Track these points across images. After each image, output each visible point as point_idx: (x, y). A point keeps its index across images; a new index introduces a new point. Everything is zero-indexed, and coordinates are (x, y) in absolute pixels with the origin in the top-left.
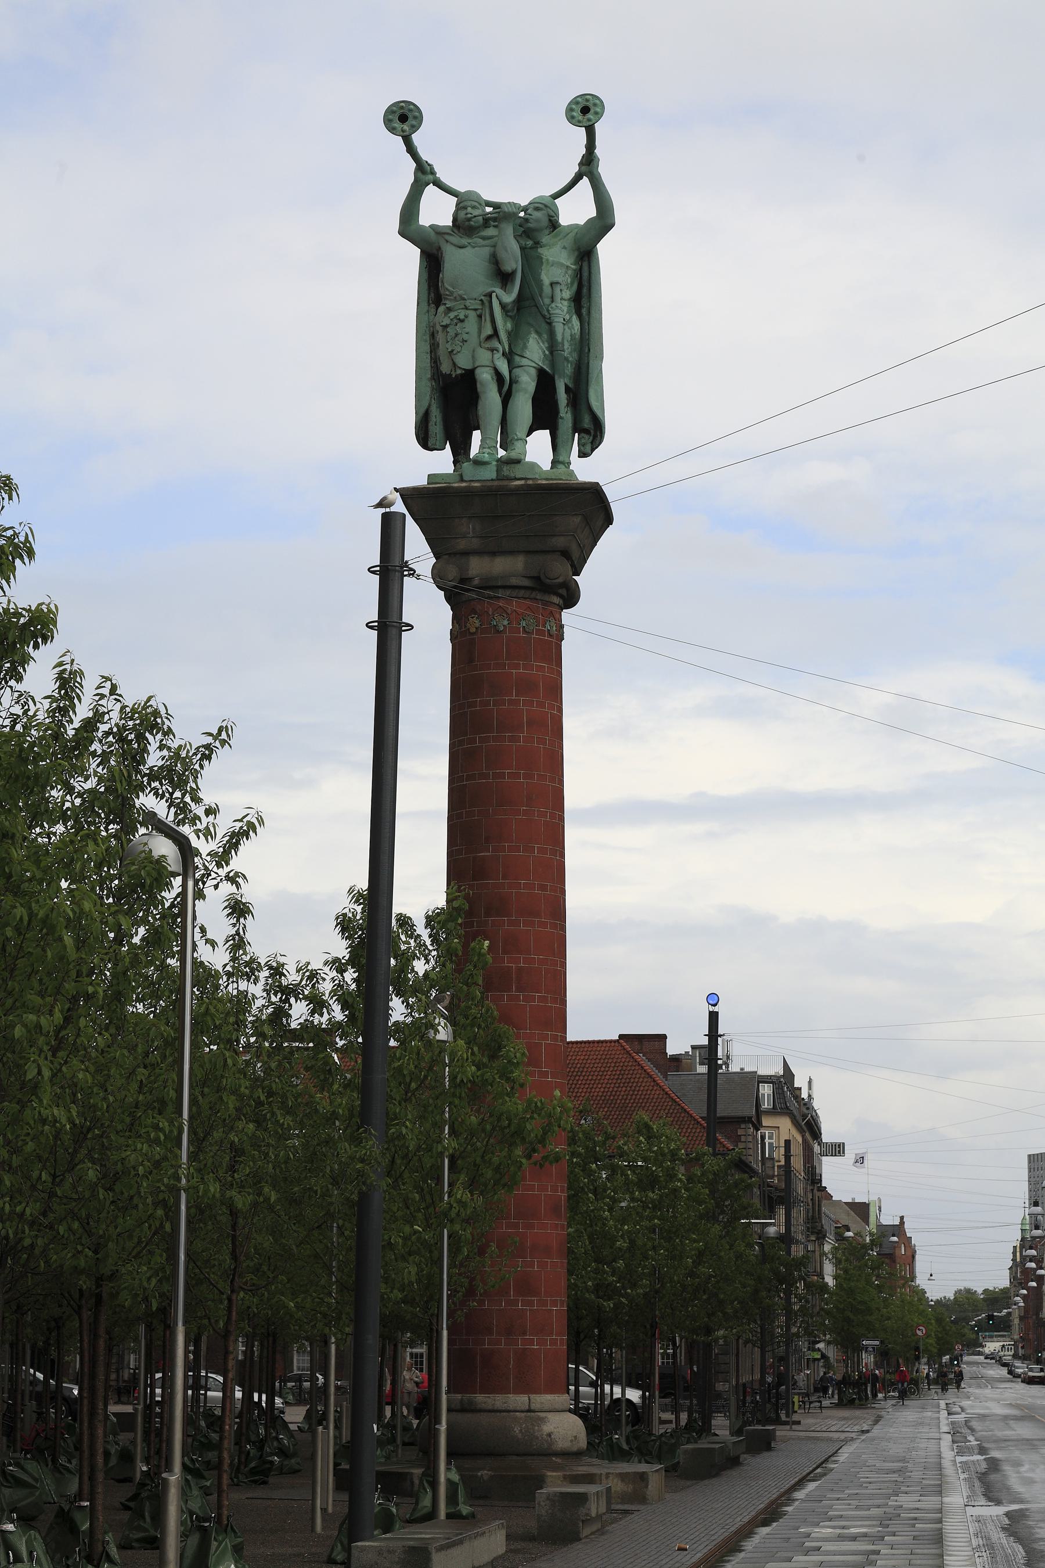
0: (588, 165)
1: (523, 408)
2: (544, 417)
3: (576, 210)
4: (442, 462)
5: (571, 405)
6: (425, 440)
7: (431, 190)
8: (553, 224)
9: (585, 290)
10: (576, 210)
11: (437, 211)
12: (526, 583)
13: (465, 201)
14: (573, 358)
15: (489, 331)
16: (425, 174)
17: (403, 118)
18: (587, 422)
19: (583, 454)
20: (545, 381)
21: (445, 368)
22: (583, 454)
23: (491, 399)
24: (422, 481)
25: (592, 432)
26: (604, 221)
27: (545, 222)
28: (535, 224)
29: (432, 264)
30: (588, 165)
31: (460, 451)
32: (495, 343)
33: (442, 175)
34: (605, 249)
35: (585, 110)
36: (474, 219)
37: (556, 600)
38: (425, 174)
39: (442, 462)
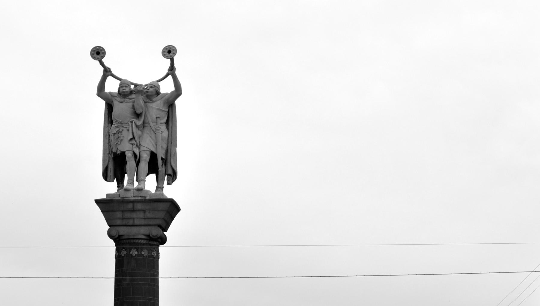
0: (172, 70)
1: (144, 166)
2: (153, 168)
3: (167, 87)
4: (112, 188)
5: (163, 165)
6: (106, 177)
7: (110, 78)
8: (158, 93)
9: (170, 119)
10: (167, 87)
11: (112, 86)
12: (143, 237)
13: (124, 84)
14: (165, 146)
15: (131, 137)
16: (107, 72)
17: (98, 53)
18: (170, 172)
19: (169, 184)
20: (153, 156)
21: (114, 150)
22: (169, 184)
23: (131, 163)
24: (104, 197)
25: (173, 176)
26: (178, 92)
27: (155, 93)
28: (151, 92)
29: (109, 108)
30: (172, 70)
31: (120, 183)
32: (133, 142)
33: (114, 72)
34: (178, 102)
35: (169, 52)
36: (127, 91)
37: (156, 243)
38: (107, 72)
39: (112, 188)
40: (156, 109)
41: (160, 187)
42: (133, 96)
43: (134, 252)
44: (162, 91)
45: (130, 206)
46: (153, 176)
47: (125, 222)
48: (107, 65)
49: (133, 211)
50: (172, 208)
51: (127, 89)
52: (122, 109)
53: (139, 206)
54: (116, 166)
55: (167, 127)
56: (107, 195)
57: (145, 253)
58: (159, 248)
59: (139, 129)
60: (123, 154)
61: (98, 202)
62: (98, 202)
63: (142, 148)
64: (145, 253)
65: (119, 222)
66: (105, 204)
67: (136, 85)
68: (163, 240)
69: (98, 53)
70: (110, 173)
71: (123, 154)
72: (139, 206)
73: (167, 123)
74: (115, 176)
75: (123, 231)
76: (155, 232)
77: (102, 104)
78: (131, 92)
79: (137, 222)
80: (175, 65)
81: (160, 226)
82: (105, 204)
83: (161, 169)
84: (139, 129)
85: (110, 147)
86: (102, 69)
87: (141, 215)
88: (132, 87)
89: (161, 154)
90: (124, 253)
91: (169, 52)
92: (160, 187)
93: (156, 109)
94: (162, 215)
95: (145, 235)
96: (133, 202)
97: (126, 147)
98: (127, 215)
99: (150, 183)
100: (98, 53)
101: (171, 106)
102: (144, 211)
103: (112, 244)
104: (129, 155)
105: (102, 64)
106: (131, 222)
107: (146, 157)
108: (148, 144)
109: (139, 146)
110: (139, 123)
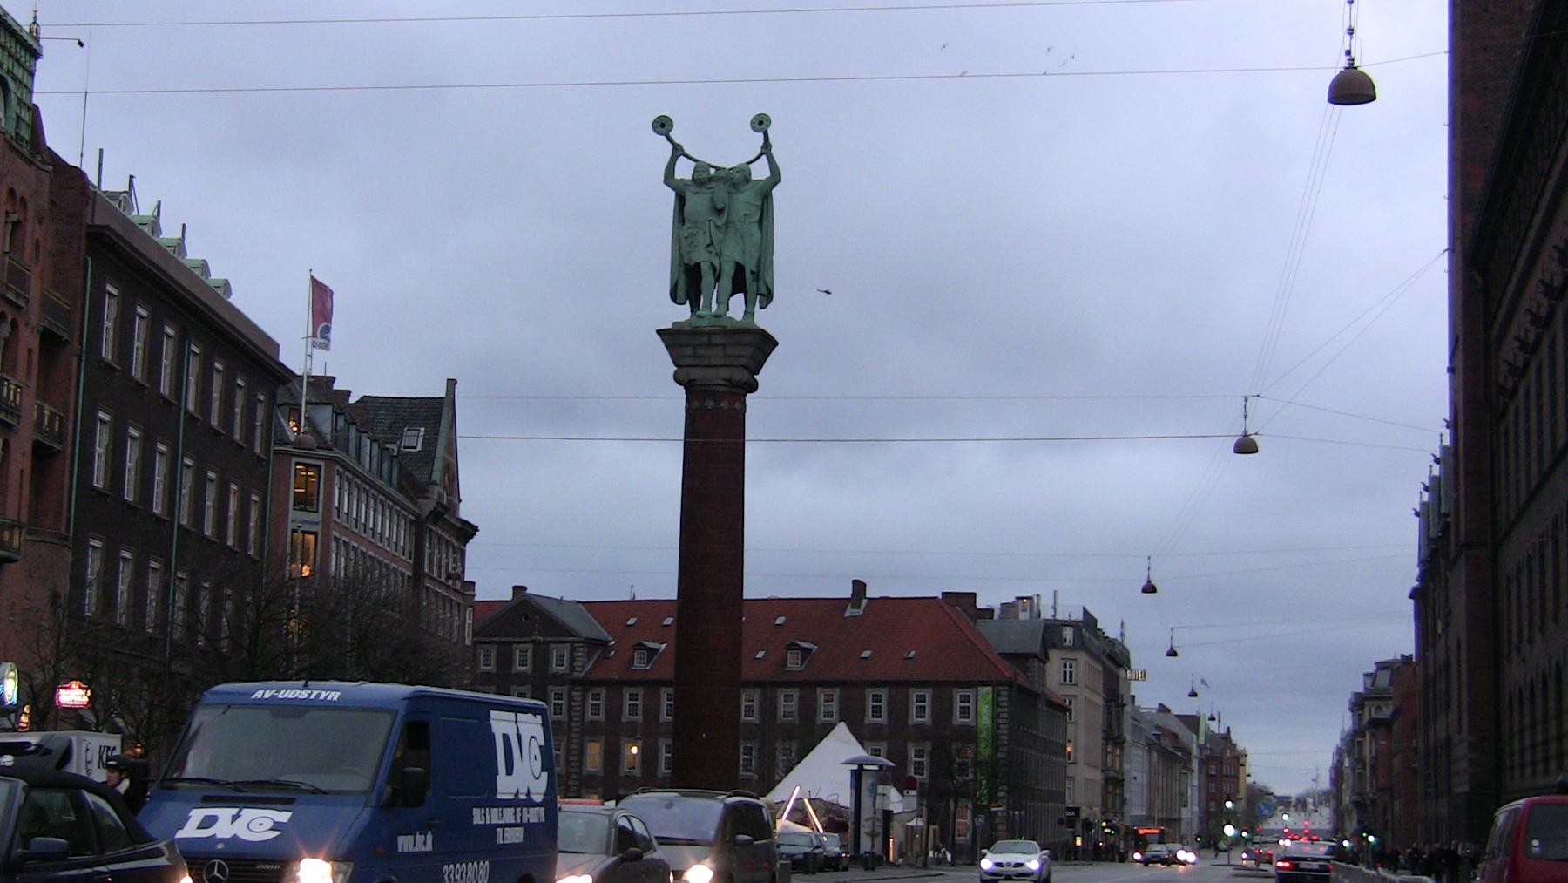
0: (767, 145)
1: (726, 282)
2: (738, 286)
3: (760, 171)
4: (683, 313)
5: (753, 281)
6: (674, 297)
7: (681, 160)
8: (747, 180)
10: (760, 171)
11: (684, 170)
13: (701, 167)
16: (678, 151)
17: (663, 126)
18: (764, 290)
20: (740, 268)
23: (707, 278)
25: (767, 297)
26: (775, 178)
28: (737, 179)
29: (681, 200)
30: (767, 145)
31: (695, 307)
33: (687, 150)
35: (761, 123)
36: (705, 178)
38: (678, 151)
39: (683, 313)
40: (744, 202)
41: (749, 312)
42: (713, 185)
43: (710, 404)
44: (754, 177)
45: (705, 339)
46: (740, 297)
47: (697, 362)
48: (677, 141)
49: (710, 345)
50: (766, 343)
51: (705, 175)
52: (698, 203)
53: (716, 339)
54: (688, 283)
55: (761, 228)
57: (724, 405)
59: (722, 231)
60: (698, 265)
61: (658, 332)
62: (658, 332)
63: (724, 258)
64: (724, 405)
65: (690, 361)
67: (717, 169)
68: (753, 387)
69: (663, 125)
70: (681, 293)
71: (698, 265)
72: (716, 339)
73: (760, 221)
74: (688, 297)
75: (696, 374)
76: (741, 375)
77: (671, 195)
78: (711, 179)
79: (714, 362)
80: (771, 140)
81: (746, 367)
83: (751, 286)
84: (722, 231)
85: (681, 256)
86: (671, 147)
87: (720, 351)
88: (712, 171)
89: (750, 266)
90: (696, 404)
91: (761, 123)
92: (749, 312)
93: (744, 202)
94: (748, 351)
96: (709, 333)
97: (700, 256)
98: (701, 352)
99: (737, 307)
100: (663, 125)
101: (766, 197)
102: (723, 345)
103: (682, 389)
104: (705, 267)
105: (670, 139)
106: (706, 362)
107: (728, 271)
108: (733, 252)
109: (719, 255)
110: (721, 222)
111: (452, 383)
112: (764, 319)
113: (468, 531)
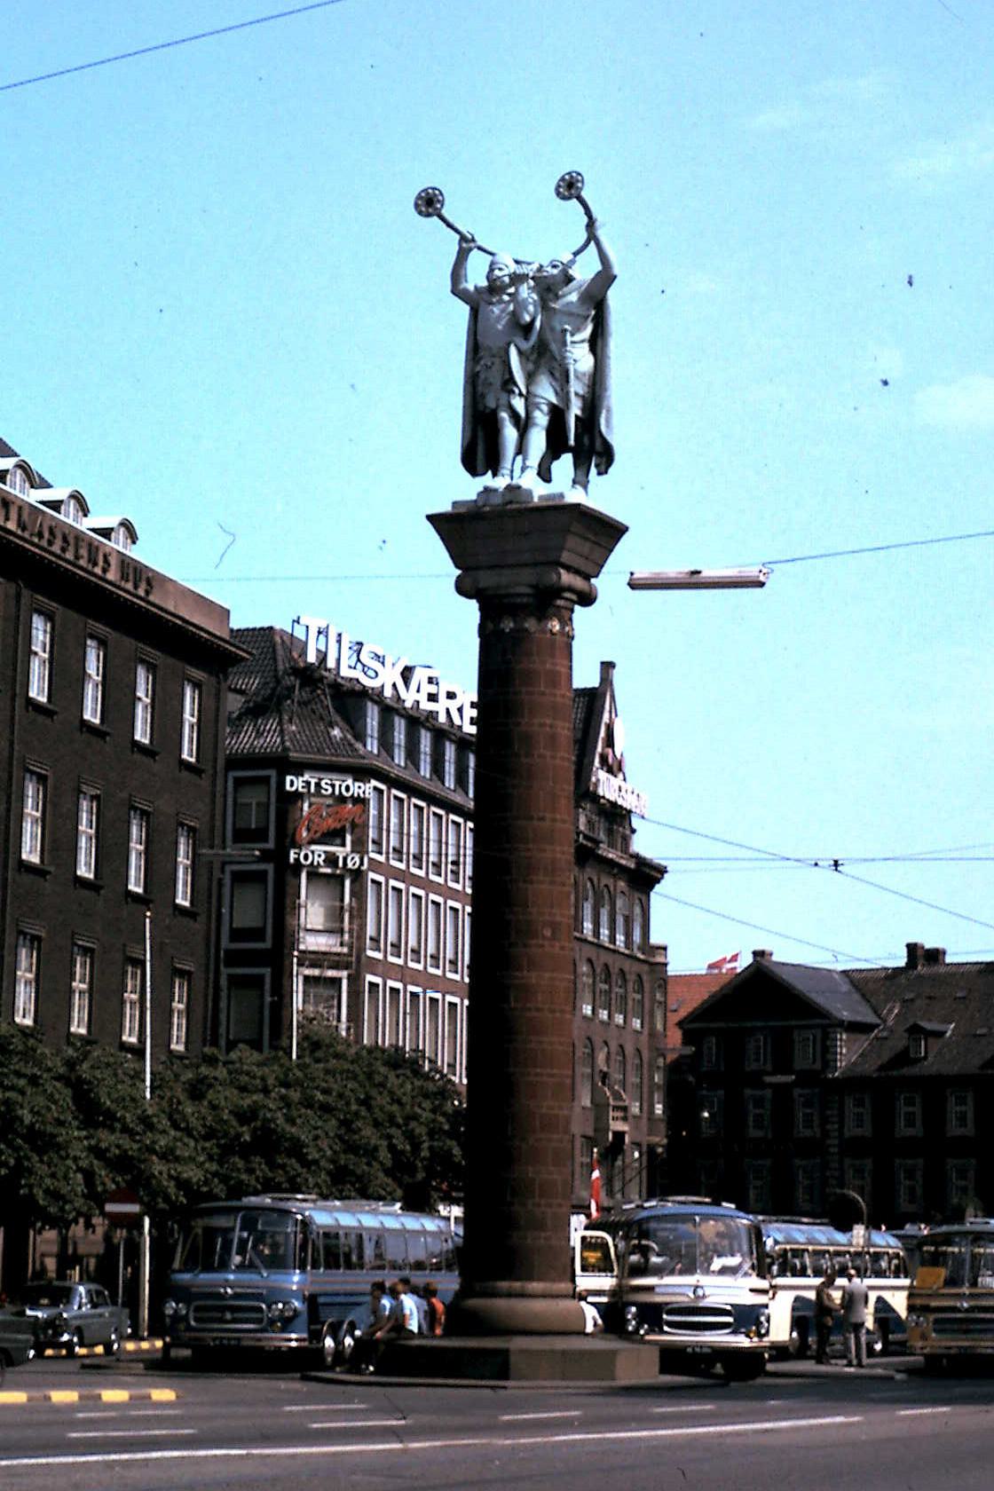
1: (538, 441)
7: (475, 254)
12: (528, 591)
16: (466, 245)
19: (599, 474)
22: (599, 474)
24: (446, 507)
26: (606, 277)
38: (466, 245)
39: (468, 488)
55: (593, 349)
56: (455, 504)
58: (575, 616)
61: (430, 518)
62: (430, 518)
66: (454, 527)
75: (487, 579)
77: (465, 309)
82: (454, 527)
95: (531, 586)
103: (472, 607)
111: (607, 667)
112: (601, 495)
113: (646, 876)
